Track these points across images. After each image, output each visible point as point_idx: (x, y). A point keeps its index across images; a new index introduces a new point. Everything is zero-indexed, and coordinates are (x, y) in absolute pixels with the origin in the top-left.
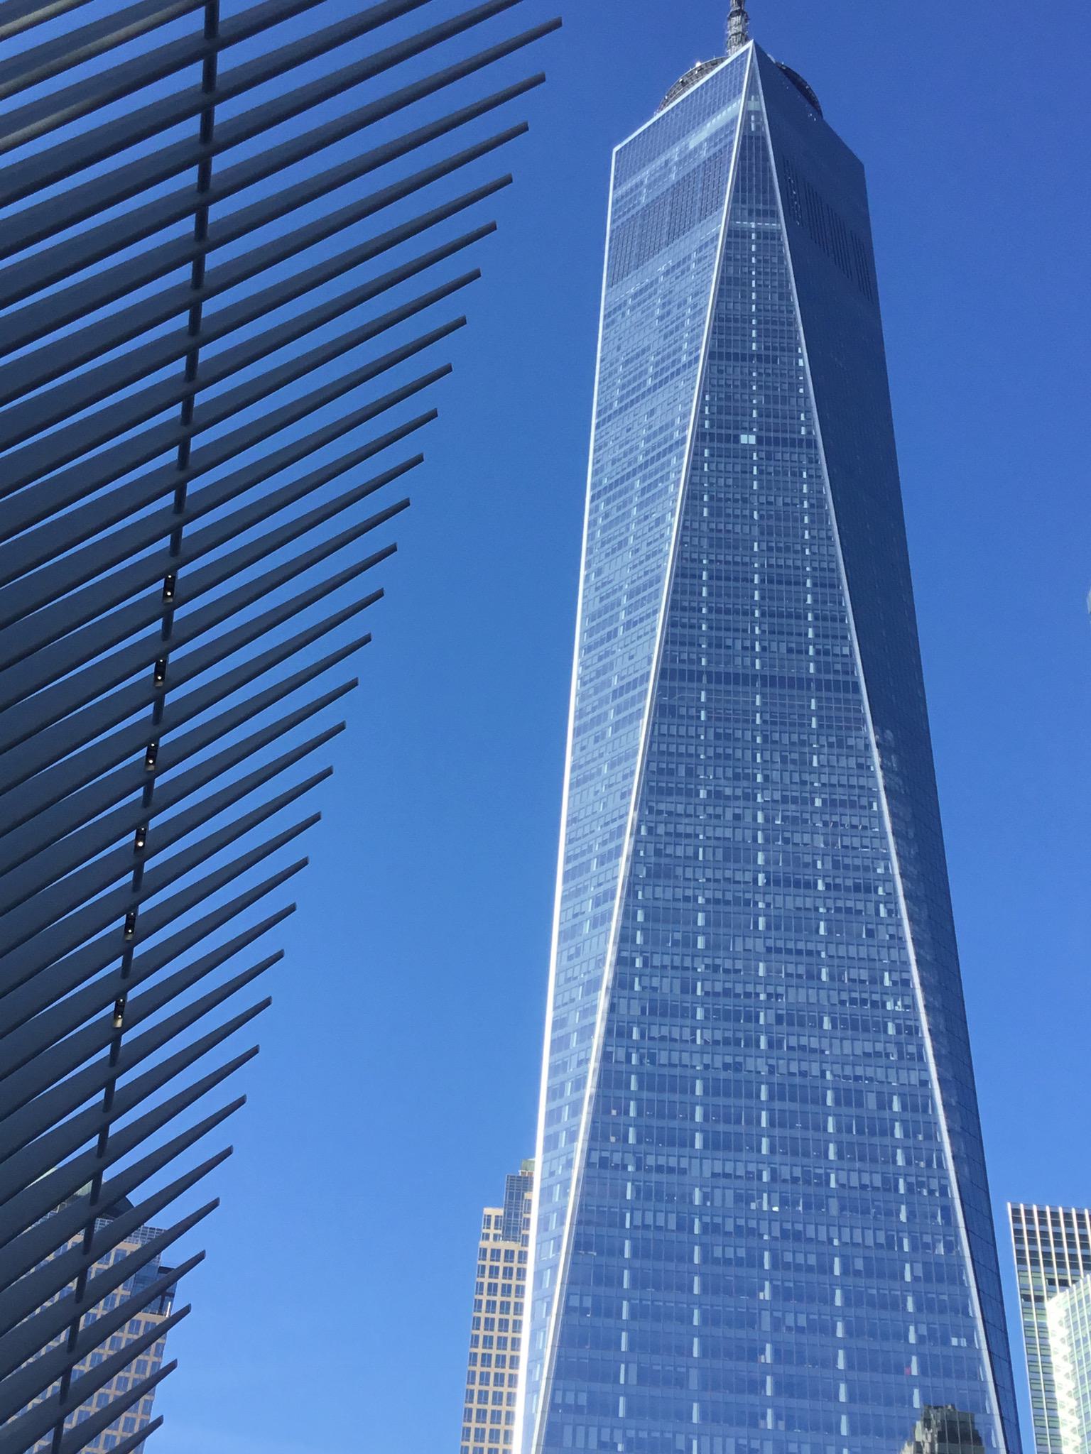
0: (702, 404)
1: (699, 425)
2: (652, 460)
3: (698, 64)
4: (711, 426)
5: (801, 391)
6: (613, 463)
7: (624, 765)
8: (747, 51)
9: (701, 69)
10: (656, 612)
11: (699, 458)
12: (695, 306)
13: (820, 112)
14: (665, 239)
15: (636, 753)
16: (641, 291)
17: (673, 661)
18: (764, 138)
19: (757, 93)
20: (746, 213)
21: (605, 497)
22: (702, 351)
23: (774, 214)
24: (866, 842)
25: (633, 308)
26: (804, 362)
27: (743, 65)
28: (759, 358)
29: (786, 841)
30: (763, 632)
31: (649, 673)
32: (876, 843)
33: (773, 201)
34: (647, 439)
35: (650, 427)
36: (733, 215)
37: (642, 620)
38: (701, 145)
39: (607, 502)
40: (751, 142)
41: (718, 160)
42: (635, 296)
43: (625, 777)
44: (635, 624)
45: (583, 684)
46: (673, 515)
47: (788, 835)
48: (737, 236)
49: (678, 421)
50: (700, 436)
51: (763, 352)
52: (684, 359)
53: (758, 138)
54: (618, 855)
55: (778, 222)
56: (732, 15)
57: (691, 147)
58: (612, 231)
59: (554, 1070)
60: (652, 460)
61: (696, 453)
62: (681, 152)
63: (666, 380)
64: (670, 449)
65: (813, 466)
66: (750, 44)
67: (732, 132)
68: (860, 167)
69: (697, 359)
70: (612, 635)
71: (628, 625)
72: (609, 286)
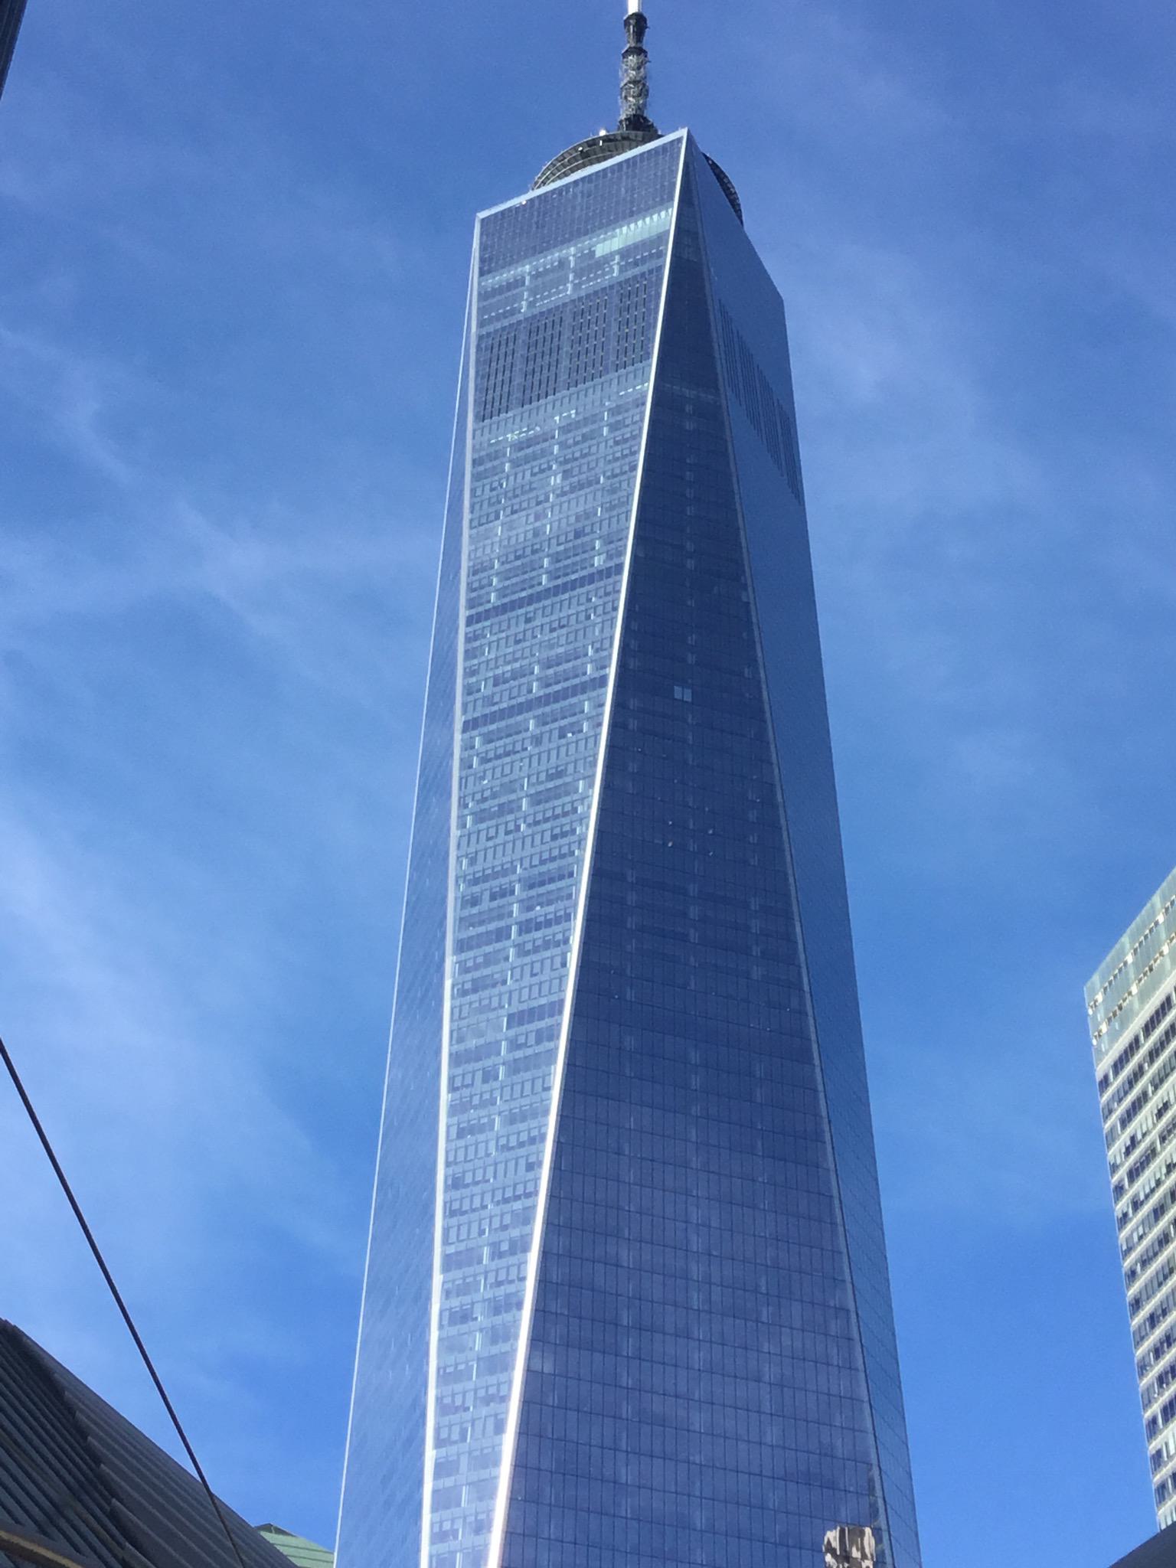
2: (557, 697)
3: (603, 133)
7: (534, 1123)
9: (606, 139)
10: (568, 917)
12: (613, 491)
15: (547, 1112)
16: (530, 442)
21: (485, 730)
25: (515, 464)
31: (562, 1002)
34: (547, 664)
35: (551, 647)
38: (612, 255)
39: (488, 739)
42: (519, 446)
43: (532, 1141)
52: (598, 561)
54: (526, 1249)
57: (598, 254)
59: (438, 1537)
60: (557, 697)
63: (573, 585)
69: (619, 568)
70: (502, 934)
71: (525, 927)
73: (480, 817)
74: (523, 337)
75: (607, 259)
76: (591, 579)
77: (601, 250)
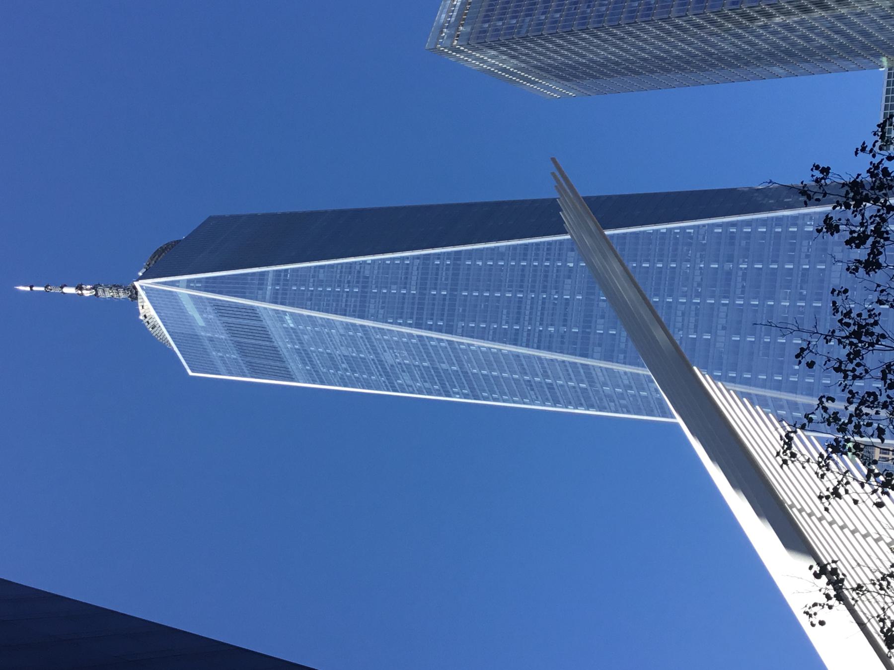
0: (394, 323)
1: (410, 325)
4: (411, 318)
5: (388, 262)
6: (426, 382)
8: (142, 287)
9: (145, 316)
11: (433, 328)
13: (178, 242)
14: (268, 343)
17: (575, 349)
18: (207, 278)
19: (172, 282)
20: (260, 292)
22: (358, 322)
23: (263, 274)
24: (701, 237)
26: (369, 258)
27: (152, 289)
28: (364, 287)
29: (699, 285)
30: (557, 292)
31: (581, 364)
32: (702, 231)
33: (253, 274)
36: (263, 300)
37: (544, 368)
40: (208, 285)
41: (218, 307)
42: (305, 364)
44: (545, 372)
45: (581, 405)
46: (473, 345)
47: (695, 285)
48: (276, 298)
49: (405, 340)
50: (418, 326)
51: (360, 285)
53: (207, 282)
55: (268, 272)
56: (96, 294)
58: (252, 377)
61: (430, 328)
62: (206, 331)
64: (424, 345)
65: (442, 257)
66: (137, 284)
67: (200, 298)
68: (210, 218)
72: (292, 379)
73: (492, 392)
74: (248, 359)
75: (205, 320)
76: (369, 339)
77: (201, 323)
